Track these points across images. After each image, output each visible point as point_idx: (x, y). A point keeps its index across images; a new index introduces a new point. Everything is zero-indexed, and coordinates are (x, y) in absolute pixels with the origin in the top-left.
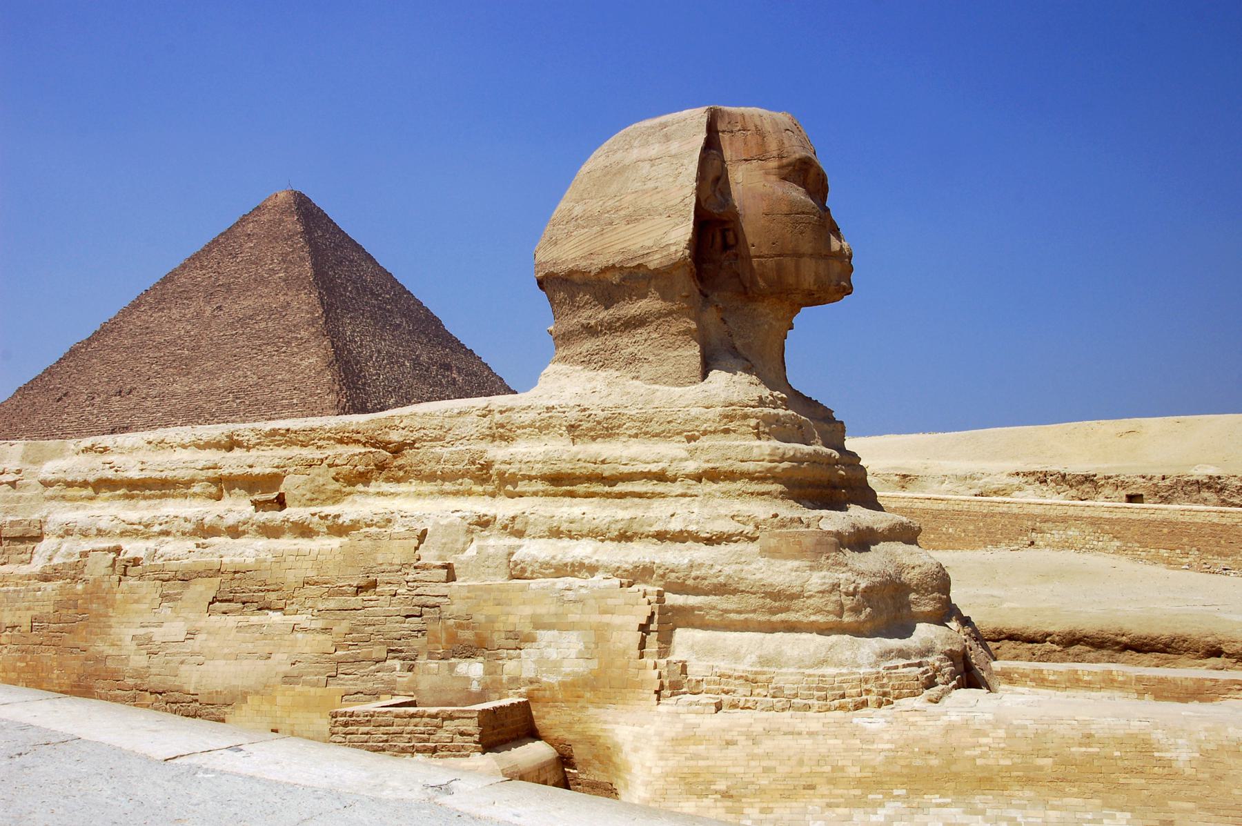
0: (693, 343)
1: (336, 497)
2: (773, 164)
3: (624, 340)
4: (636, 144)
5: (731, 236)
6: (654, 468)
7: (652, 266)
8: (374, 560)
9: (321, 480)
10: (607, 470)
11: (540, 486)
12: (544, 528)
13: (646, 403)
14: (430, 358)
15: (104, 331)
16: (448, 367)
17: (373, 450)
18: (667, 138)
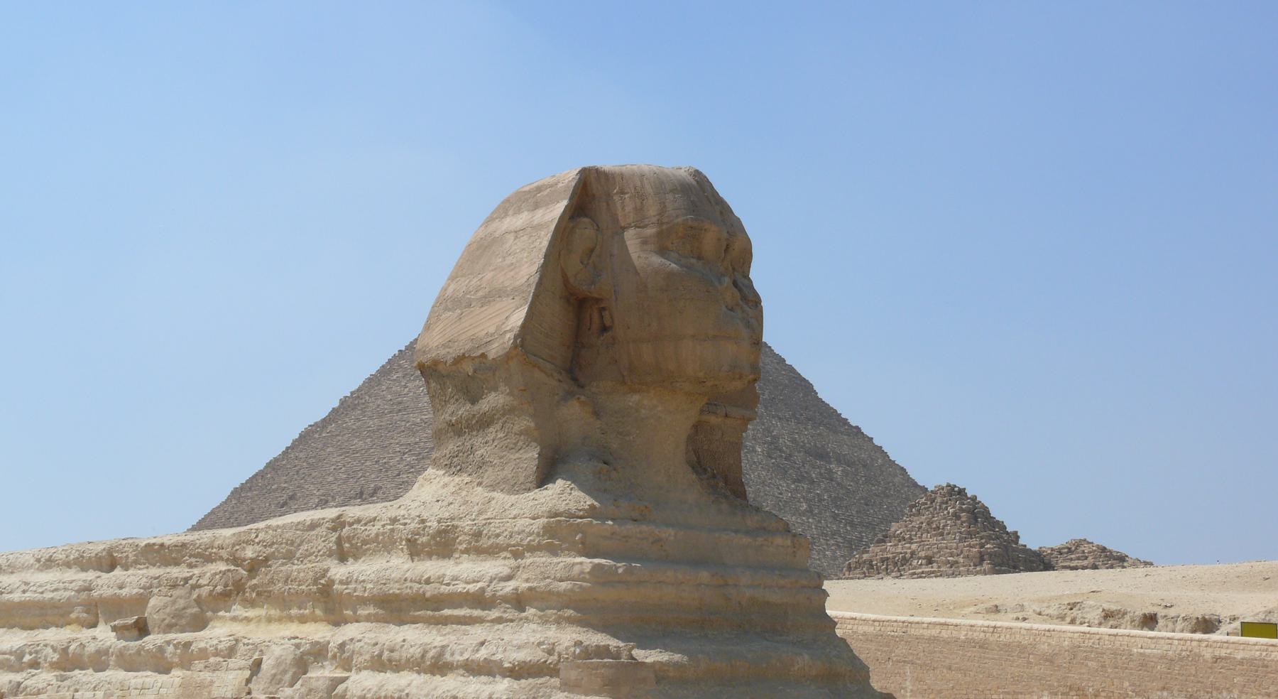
0: (534, 444)
1: (199, 623)
2: (651, 231)
3: (478, 441)
4: (511, 212)
5: (606, 314)
6: (472, 588)
7: (491, 356)
8: (209, 693)
9: (181, 603)
10: (430, 590)
11: (371, 610)
12: (367, 657)
13: (480, 513)
14: (794, 441)
15: (348, 405)
16: (822, 455)
17: (233, 568)
18: (536, 206)
